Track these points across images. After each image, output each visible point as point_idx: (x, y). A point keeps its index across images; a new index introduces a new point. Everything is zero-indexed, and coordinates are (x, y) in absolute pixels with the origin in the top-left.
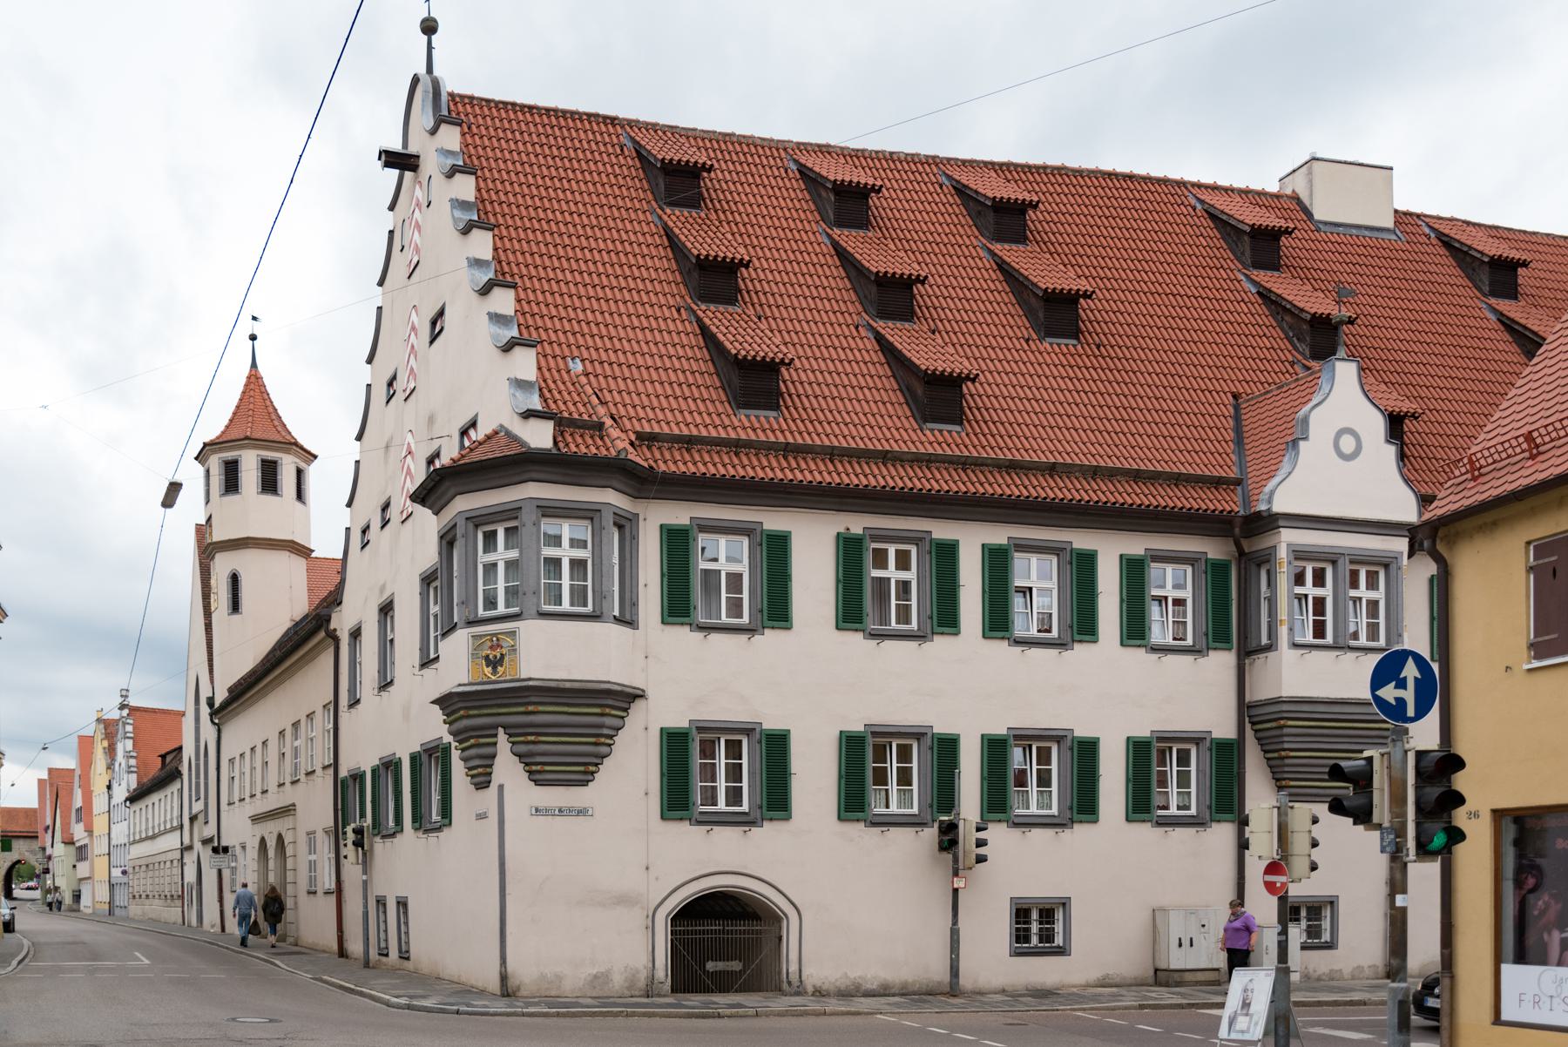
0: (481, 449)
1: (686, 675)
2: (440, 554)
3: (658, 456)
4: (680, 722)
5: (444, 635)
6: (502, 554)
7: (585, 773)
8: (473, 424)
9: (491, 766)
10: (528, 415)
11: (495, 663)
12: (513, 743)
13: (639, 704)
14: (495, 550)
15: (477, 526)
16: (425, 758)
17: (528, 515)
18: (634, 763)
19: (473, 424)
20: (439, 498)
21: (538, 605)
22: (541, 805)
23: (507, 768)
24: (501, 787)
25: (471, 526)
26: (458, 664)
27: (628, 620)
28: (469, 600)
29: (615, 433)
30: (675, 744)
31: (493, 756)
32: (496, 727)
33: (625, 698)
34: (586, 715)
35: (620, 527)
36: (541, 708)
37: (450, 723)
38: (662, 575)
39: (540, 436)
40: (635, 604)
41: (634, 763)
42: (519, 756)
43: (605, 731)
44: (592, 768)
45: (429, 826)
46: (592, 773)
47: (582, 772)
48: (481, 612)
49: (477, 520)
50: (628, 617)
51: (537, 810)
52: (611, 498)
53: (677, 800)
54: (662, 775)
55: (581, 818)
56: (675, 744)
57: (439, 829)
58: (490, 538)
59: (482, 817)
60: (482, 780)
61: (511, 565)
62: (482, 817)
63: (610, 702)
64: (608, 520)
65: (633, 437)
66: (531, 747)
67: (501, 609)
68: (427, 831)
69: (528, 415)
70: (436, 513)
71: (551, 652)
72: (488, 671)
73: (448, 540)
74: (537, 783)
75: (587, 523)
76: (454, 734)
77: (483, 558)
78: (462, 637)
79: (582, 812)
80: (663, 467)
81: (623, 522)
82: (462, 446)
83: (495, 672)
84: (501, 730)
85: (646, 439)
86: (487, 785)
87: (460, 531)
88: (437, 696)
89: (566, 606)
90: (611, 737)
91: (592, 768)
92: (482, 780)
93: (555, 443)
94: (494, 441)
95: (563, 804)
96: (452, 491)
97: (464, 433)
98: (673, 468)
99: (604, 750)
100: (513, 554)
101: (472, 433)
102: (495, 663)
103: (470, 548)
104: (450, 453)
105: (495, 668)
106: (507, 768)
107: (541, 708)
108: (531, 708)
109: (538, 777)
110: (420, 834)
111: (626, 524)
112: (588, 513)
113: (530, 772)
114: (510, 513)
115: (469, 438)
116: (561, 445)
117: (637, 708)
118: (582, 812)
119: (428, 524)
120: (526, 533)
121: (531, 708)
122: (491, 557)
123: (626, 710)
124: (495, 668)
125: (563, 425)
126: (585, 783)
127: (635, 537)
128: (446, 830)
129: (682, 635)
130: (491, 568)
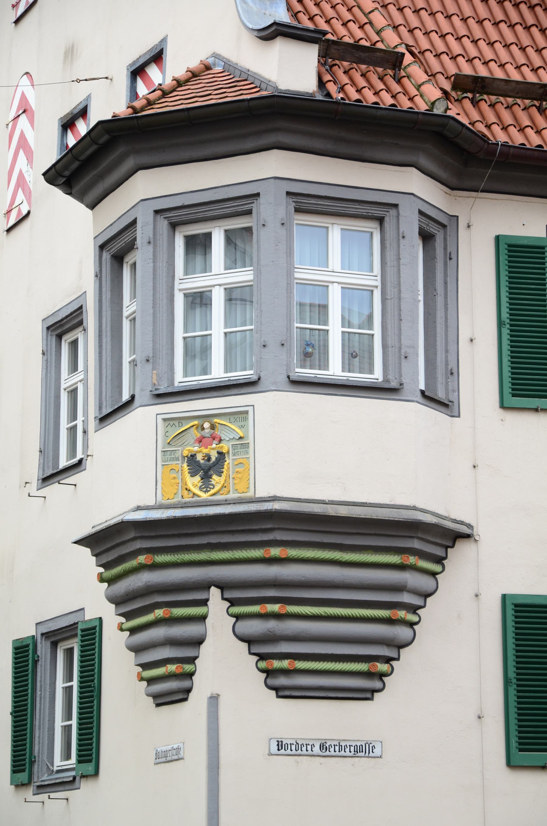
0: (181, 92)
2: (99, 276)
3: (491, 118)
5: (104, 419)
6: (219, 273)
7: (369, 675)
8: (157, 57)
9: (192, 660)
10: (272, 33)
11: (207, 470)
12: (238, 617)
13: (462, 547)
14: (206, 268)
15: (174, 226)
16: (43, 648)
17: (271, 209)
19: (157, 57)
20: (101, 177)
21: (289, 366)
22: (288, 736)
23: (224, 660)
24: (214, 700)
25: (163, 224)
27: (441, 402)
28: (158, 356)
29: (417, 72)
31: (198, 642)
32: (205, 586)
33: (429, 540)
34: (369, 569)
35: (426, 237)
36: (293, 553)
37: (111, 581)
38: (500, 324)
39: (294, 70)
40: (453, 373)
42: (249, 641)
43: (407, 598)
44: (383, 667)
45: (46, 778)
46: (381, 676)
47: (364, 675)
48: (180, 380)
49: (177, 216)
50: (441, 395)
51: (280, 745)
52: (412, 185)
54: (507, 682)
55: (362, 762)
57: (70, 784)
58: (199, 245)
59: (168, 758)
60: (171, 687)
61: (235, 297)
62: (168, 758)
63: (416, 544)
64: (410, 224)
65: (447, 86)
66: (272, 625)
67: (218, 372)
68: (42, 788)
69: (272, 33)
70: (92, 206)
71: (309, 452)
73: (116, 250)
74: (281, 692)
75: (372, 226)
76: (117, 601)
77: (186, 282)
78: (144, 420)
79: (363, 750)
80: (502, 137)
81: (433, 228)
82: (134, 95)
84: (215, 593)
85: (472, 87)
86: (182, 695)
87: (142, 234)
88: (86, 530)
89: (335, 370)
90: (414, 609)
91: (383, 667)
92: (171, 687)
93: (321, 84)
94: (205, 80)
95: (329, 734)
96: (130, 163)
97: (138, 72)
98: (518, 139)
99: (403, 632)
100: (243, 276)
101: (153, 72)
102: (207, 470)
103: (162, 264)
104: (110, 103)
105: (206, 478)
106: (224, 660)
107: (293, 553)
108: (275, 552)
109: (282, 681)
110: (29, 794)
111: (435, 233)
112: (375, 211)
113: (269, 673)
114: (238, 205)
115: (148, 81)
116: (332, 88)
117: (460, 556)
118: (363, 750)
119: (72, 228)
120: (266, 239)
121: (275, 552)
122: (198, 282)
123: (440, 560)
124: (206, 478)
125: (332, 52)
126: (367, 694)
127: (451, 257)
128: (86, 786)
130: (199, 300)
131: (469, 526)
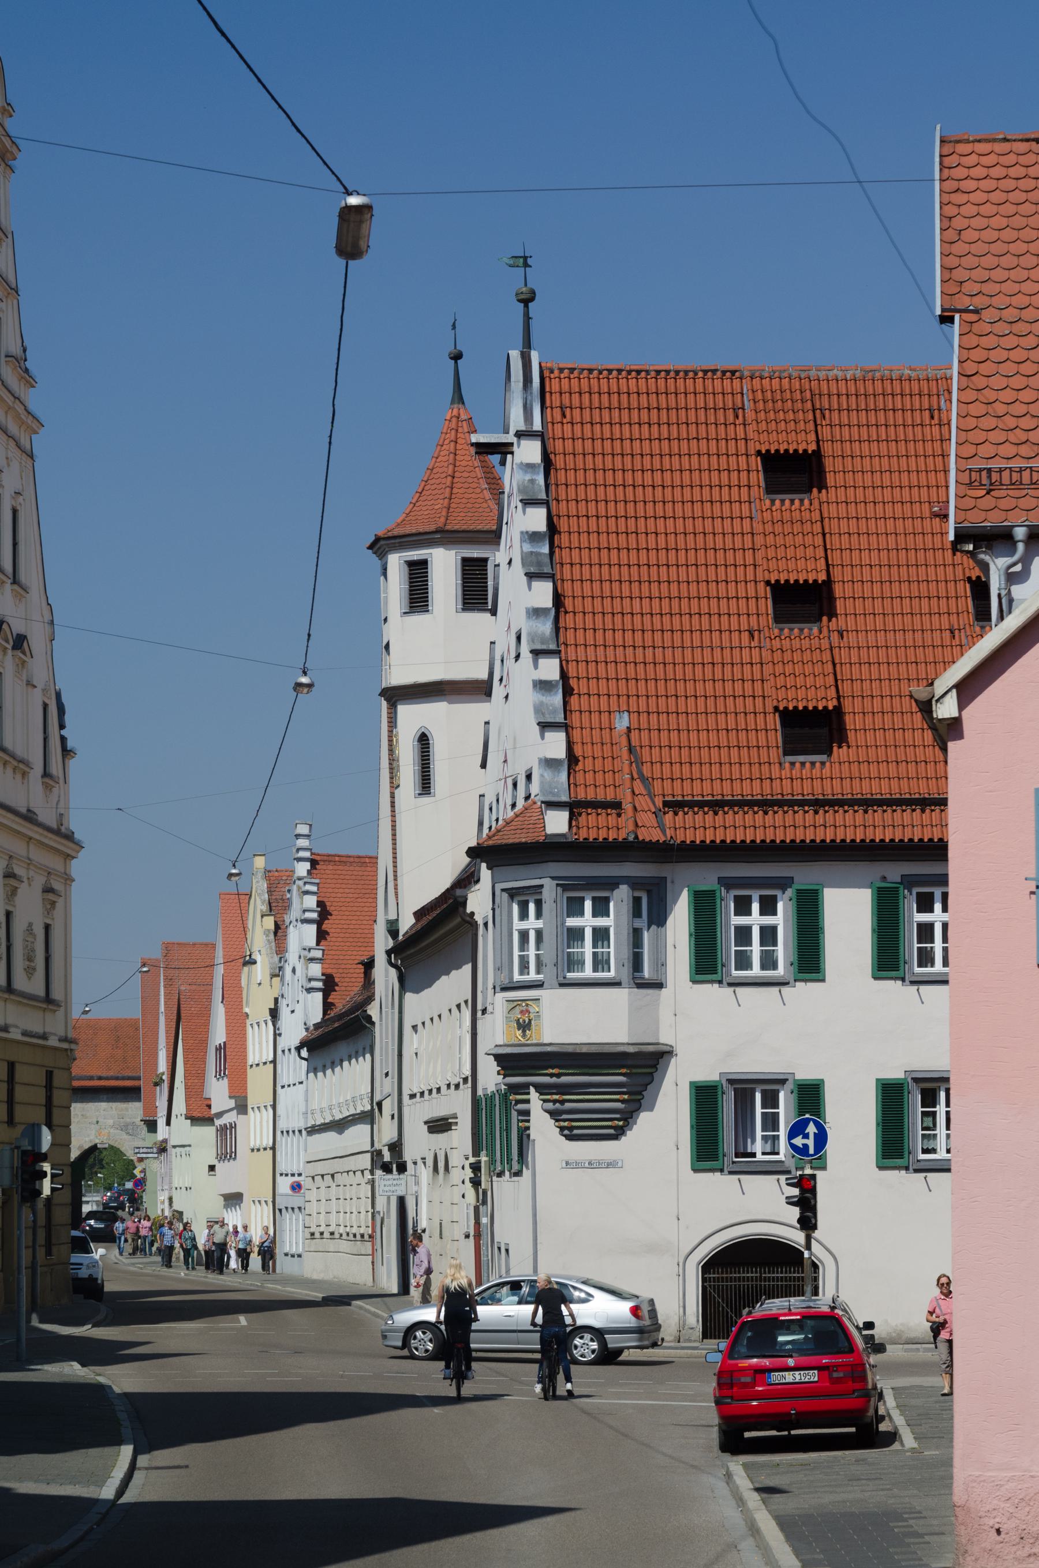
1: (711, 1030)
4: (709, 1075)
11: (524, 1027)
18: (666, 1121)
26: (497, 1032)
30: (705, 1096)
41: (666, 1121)
48: (517, 977)
53: (707, 1152)
56: (705, 1096)
72: (519, 1033)
77: (518, 925)
83: (524, 1035)
102: (524, 1027)
105: (524, 1032)
113: (562, 1129)
124: (524, 1032)
126: (615, 1137)
129: (711, 992)
131: (671, 1046)
